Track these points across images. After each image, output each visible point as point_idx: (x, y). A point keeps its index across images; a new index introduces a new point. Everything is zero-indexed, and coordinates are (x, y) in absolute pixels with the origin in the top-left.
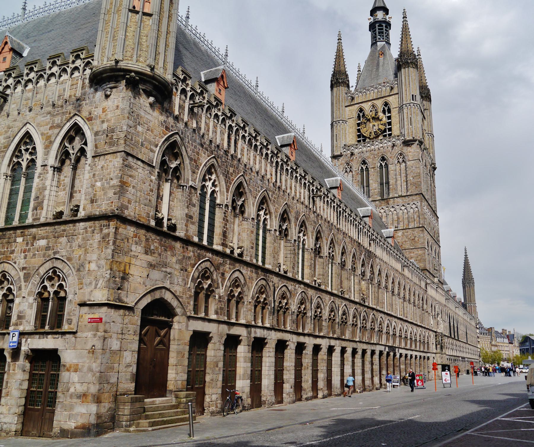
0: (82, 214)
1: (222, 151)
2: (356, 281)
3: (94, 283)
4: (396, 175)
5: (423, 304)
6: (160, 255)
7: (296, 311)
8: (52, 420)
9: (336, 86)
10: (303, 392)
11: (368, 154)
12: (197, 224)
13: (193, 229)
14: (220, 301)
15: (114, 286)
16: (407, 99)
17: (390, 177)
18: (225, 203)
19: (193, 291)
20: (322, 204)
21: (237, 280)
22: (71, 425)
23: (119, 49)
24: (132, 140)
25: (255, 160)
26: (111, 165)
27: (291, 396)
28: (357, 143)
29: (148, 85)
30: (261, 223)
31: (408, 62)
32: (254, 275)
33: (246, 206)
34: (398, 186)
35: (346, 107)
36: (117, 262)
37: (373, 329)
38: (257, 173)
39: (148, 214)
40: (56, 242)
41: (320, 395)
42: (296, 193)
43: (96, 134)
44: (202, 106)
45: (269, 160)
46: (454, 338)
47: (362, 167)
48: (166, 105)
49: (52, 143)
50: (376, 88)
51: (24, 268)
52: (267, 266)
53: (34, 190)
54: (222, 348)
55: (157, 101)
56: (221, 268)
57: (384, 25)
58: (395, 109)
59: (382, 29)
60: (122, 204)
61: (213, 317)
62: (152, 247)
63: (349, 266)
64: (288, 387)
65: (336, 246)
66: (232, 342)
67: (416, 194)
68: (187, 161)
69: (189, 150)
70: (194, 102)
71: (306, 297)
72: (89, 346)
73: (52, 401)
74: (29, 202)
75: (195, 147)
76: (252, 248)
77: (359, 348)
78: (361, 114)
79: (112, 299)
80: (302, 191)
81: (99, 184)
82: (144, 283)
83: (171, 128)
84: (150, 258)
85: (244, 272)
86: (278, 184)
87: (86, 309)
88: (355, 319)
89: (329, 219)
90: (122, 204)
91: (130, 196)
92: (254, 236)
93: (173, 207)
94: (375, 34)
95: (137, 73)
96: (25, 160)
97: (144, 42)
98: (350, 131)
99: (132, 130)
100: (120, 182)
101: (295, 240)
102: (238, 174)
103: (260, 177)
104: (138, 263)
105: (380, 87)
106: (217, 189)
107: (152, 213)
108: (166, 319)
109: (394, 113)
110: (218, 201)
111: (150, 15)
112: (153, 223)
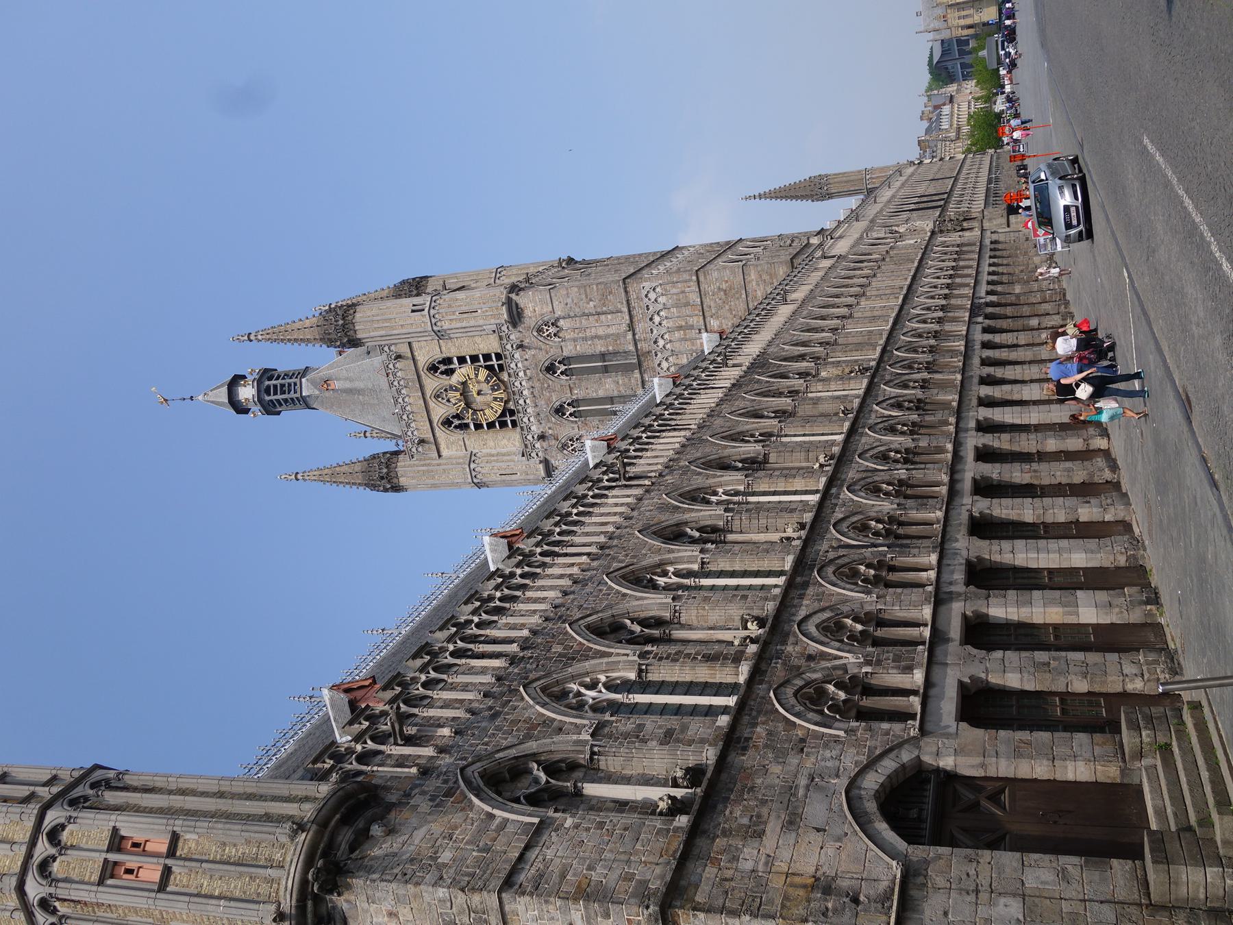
1: (510, 670)
2: (820, 388)
4: (585, 339)
5: (870, 261)
6: (764, 802)
7: (897, 501)
9: (395, 480)
10: (1096, 480)
11: (542, 403)
12: (686, 719)
13: (697, 727)
14: (879, 663)
15: (848, 913)
16: (422, 320)
17: (590, 352)
18: (636, 658)
19: (854, 724)
20: (642, 461)
21: (823, 628)
24: (473, 875)
25: (536, 600)
27: (1109, 501)
28: (518, 429)
29: (340, 838)
30: (686, 581)
31: (343, 325)
32: (811, 591)
33: (643, 615)
34: (608, 330)
35: (440, 456)
36: (783, 906)
37: (932, 350)
38: (565, 593)
39: (659, 832)
41: (1101, 443)
42: (615, 514)
44: (402, 718)
45: (538, 570)
46: (947, 201)
47: (571, 415)
48: (392, 798)
50: (398, 391)
52: (788, 564)
54: (998, 654)
55: (380, 818)
56: (796, 662)
57: (267, 383)
58: (443, 349)
59: (275, 386)
60: (633, 895)
61: (918, 676)
62: (745, 821)
63: (785, 402)
64: (1087, 510)
65: (740, 428)
66: (982, 634)
67: (626, 292)
68: (532, 746)
69: (505, 743)
70: (390, 735)
71: (862, 483)
75: (498, 729)
76: (745, 597)
77: (978, 372)
78: (457, 422)
79: (884, 918)
80: (610, 501)
82: (839, 839)
83: (451, 784)
84: (773, 826)
85: (802, 613)
86: (593, 549)
88: (911, 384)
89: (677, 446)
90: (633, 895)
91: (614, 876)
92: (716, 596)
93: (644, 776)
94: (286, 401)
97: (237, 851)
98: (492, 444)
99: (448, 875)
100: (576, 900)
101: (726, 510)
102: (567, 632)
103: (576, 588)
104: (785, 854)
105: (396, 383)
106: (603, 678)
107: (658, 823)
108: (931, 786)
109: (452, 350)
110: (632, 676)
111: (175, 838)
112: (683, 820)
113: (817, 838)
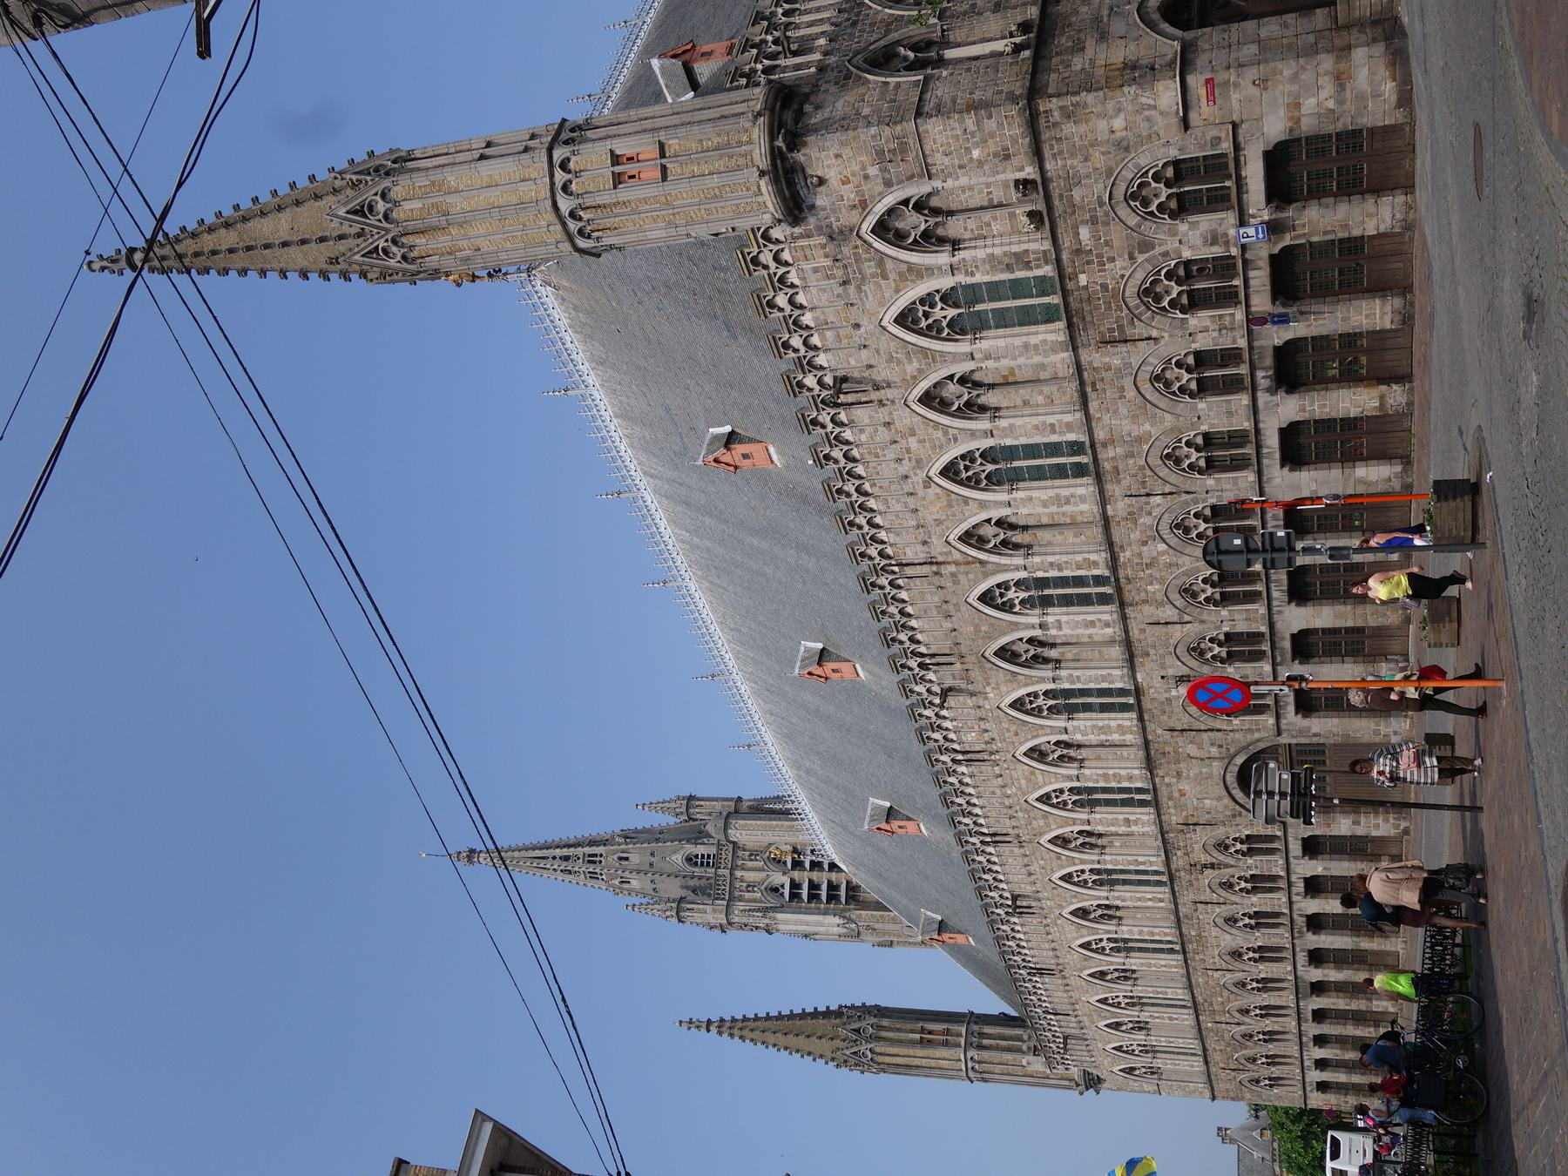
0: (1030, 172)
3: (1147, 113)
6: (1080, 31)
8: (1386, 129)
22: (1389, 88)
23: (739, 177)
26: (941, 139)
40: (1083, 207)
43: (888, 184)
49: (911, 268)
51: (1132, 257)
53: (996, 278)
68: (895, 36)
72: (1255, 91)
73: (1351, 139)
74: (1017, 280)
81: (976, 153)
84: (1090, 44)
87: (1193, 115)
95: (772, 138)
96: (944, 313)
99: (874, 120)
100: (968, 111)
111: (662, 146)
112: (1026, 54)
113: (1119, 42)
